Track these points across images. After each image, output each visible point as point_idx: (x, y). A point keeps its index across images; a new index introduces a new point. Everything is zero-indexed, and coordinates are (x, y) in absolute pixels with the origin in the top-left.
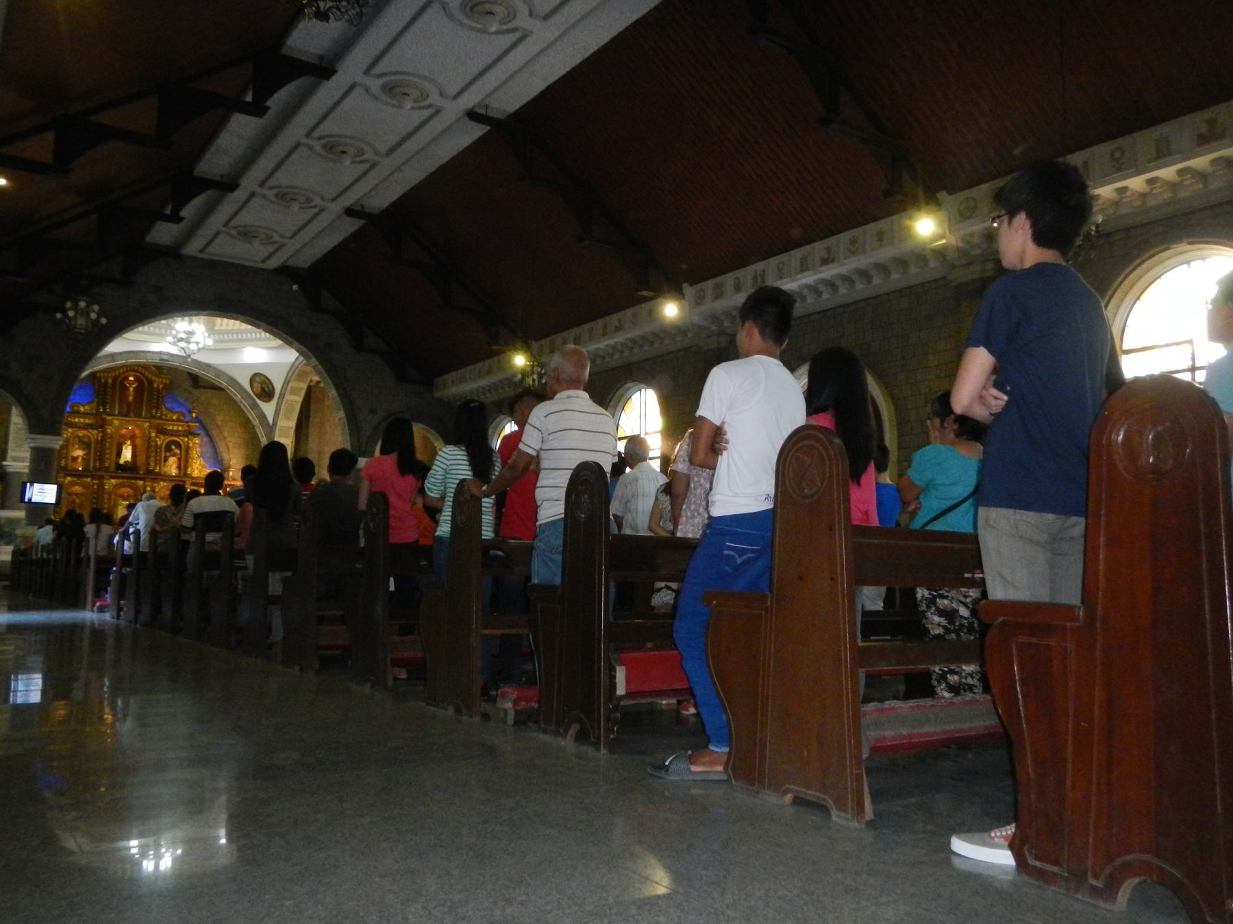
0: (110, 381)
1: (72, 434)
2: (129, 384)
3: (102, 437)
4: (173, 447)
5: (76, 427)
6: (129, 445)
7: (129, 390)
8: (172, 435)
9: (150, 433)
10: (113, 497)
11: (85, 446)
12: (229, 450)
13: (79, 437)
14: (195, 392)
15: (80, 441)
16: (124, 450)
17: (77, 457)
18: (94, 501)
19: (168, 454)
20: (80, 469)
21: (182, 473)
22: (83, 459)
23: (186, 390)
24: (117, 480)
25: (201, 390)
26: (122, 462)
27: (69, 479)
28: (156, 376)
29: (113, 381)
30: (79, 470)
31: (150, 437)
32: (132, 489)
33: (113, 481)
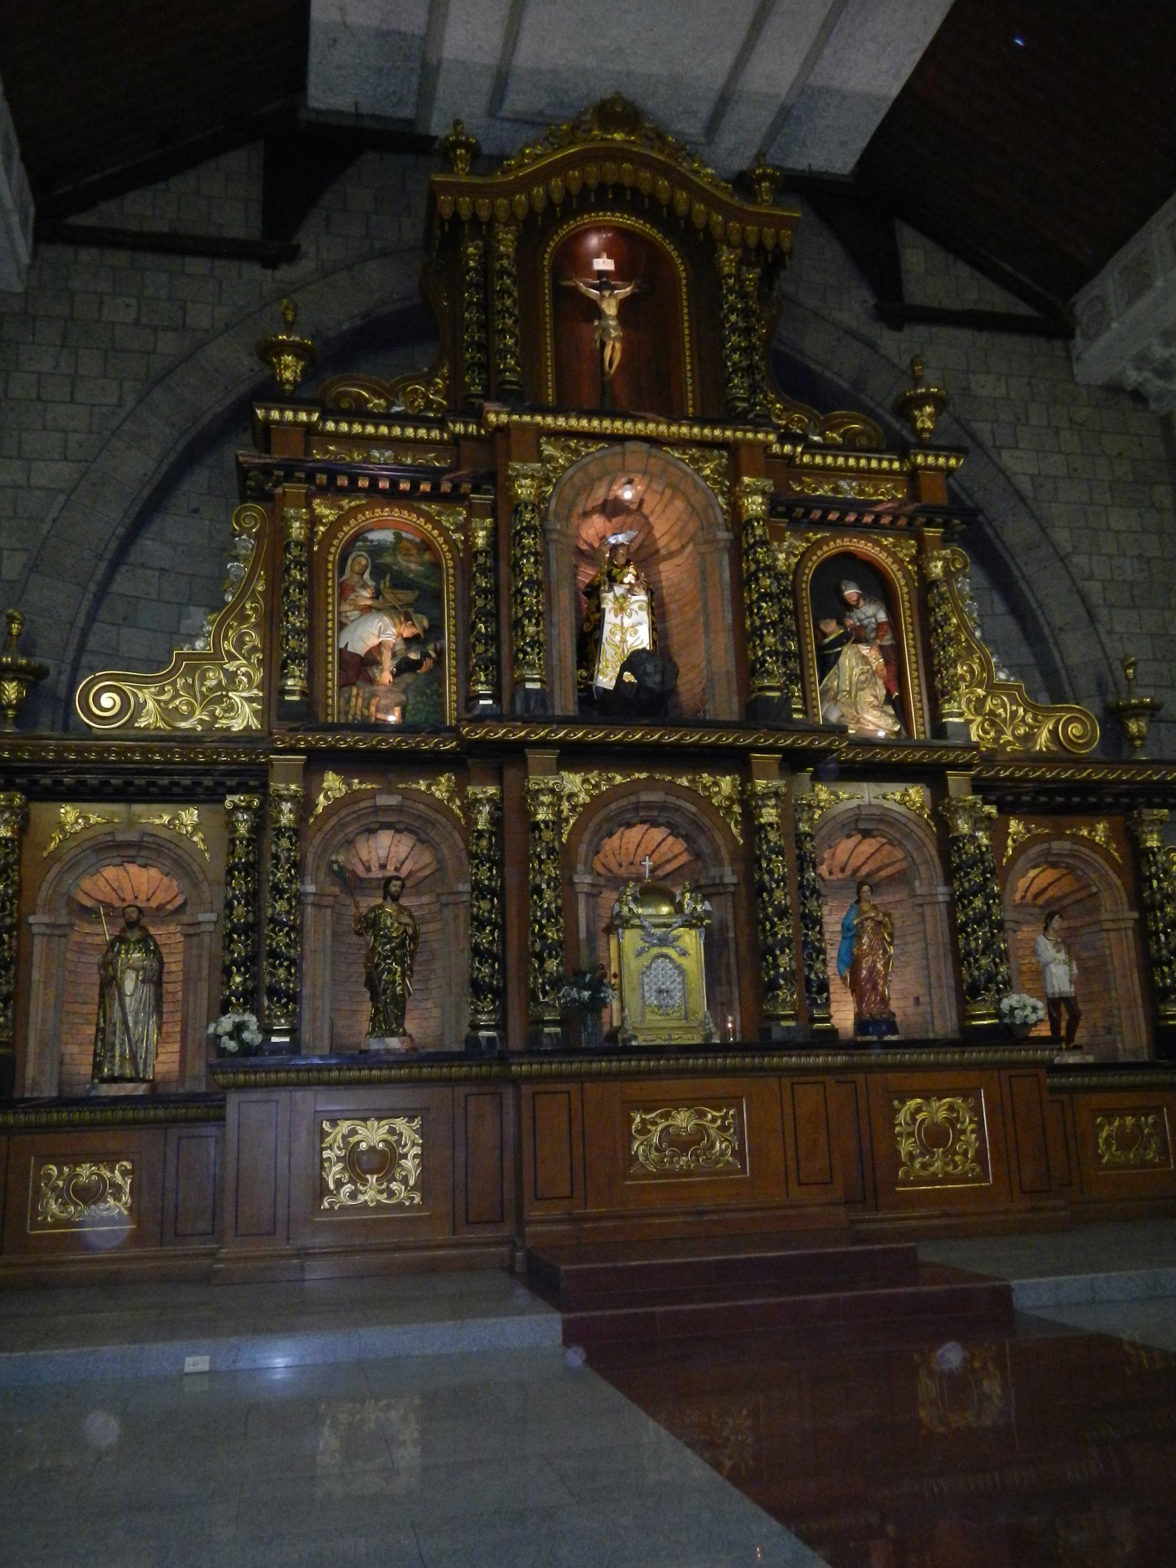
0: (506, 241)
1: (334, 528)
2: (594, 287)
3: (494, 533)
4: (851, 592)
5: (352, 490)
6: (631, 590)
7: (600, 314)
8: (840, 527)
9: (735, 508)
10: (583, 879)
11: (408, 596)
12: (1092, 618)
13: (377, 550)
14: (891, 341)
15: (378, 572)
16: (610, 618)
17: (371, 659)
18: (485, 905)
19: (832, 629)
20: (393, 718)
21: (920, 728)
22: (404, 667)
23: (850, 332)
24: (594, 777)
25: (920, 332)
26: (606, 680)
27: (332, 782)
28: (729, 212)
29: (521, 243)
30: (381, 727)
31: (738, 522)
32: (674, 830)
33: (572, 782)
